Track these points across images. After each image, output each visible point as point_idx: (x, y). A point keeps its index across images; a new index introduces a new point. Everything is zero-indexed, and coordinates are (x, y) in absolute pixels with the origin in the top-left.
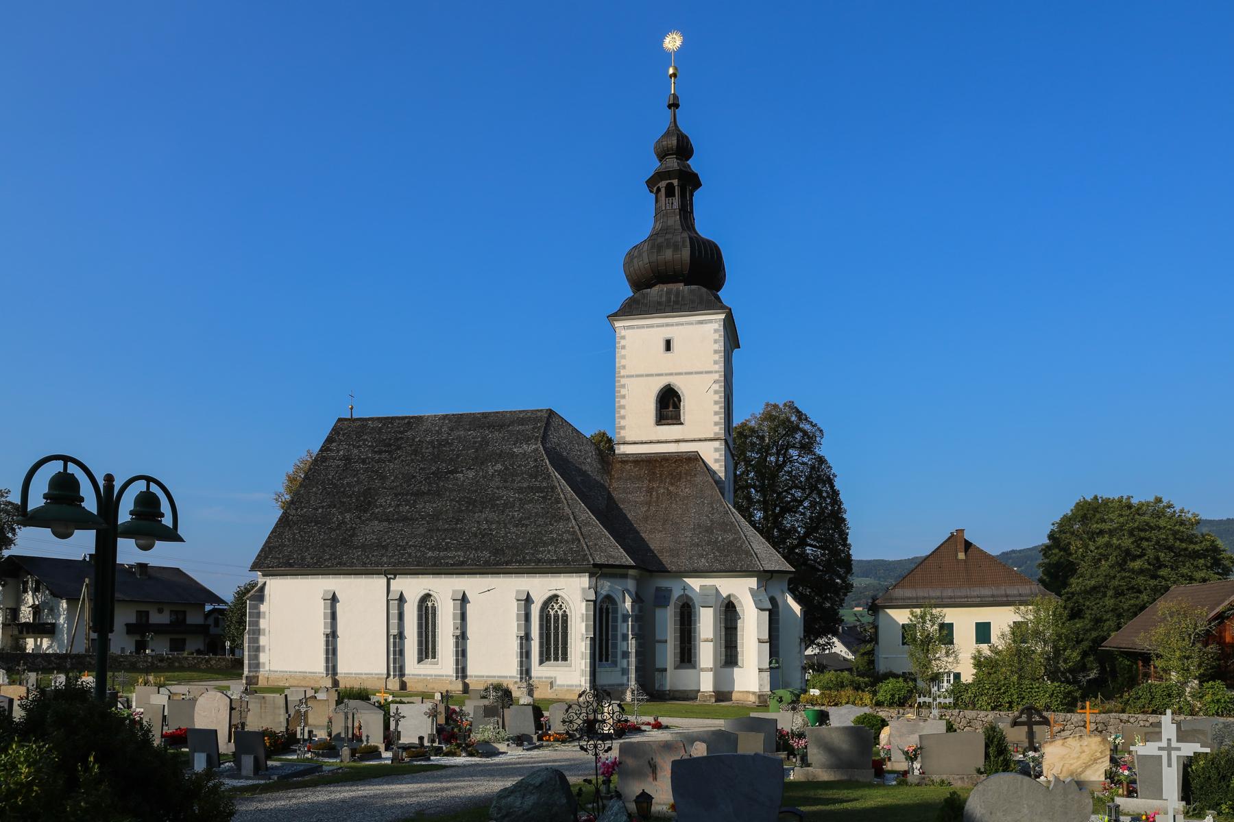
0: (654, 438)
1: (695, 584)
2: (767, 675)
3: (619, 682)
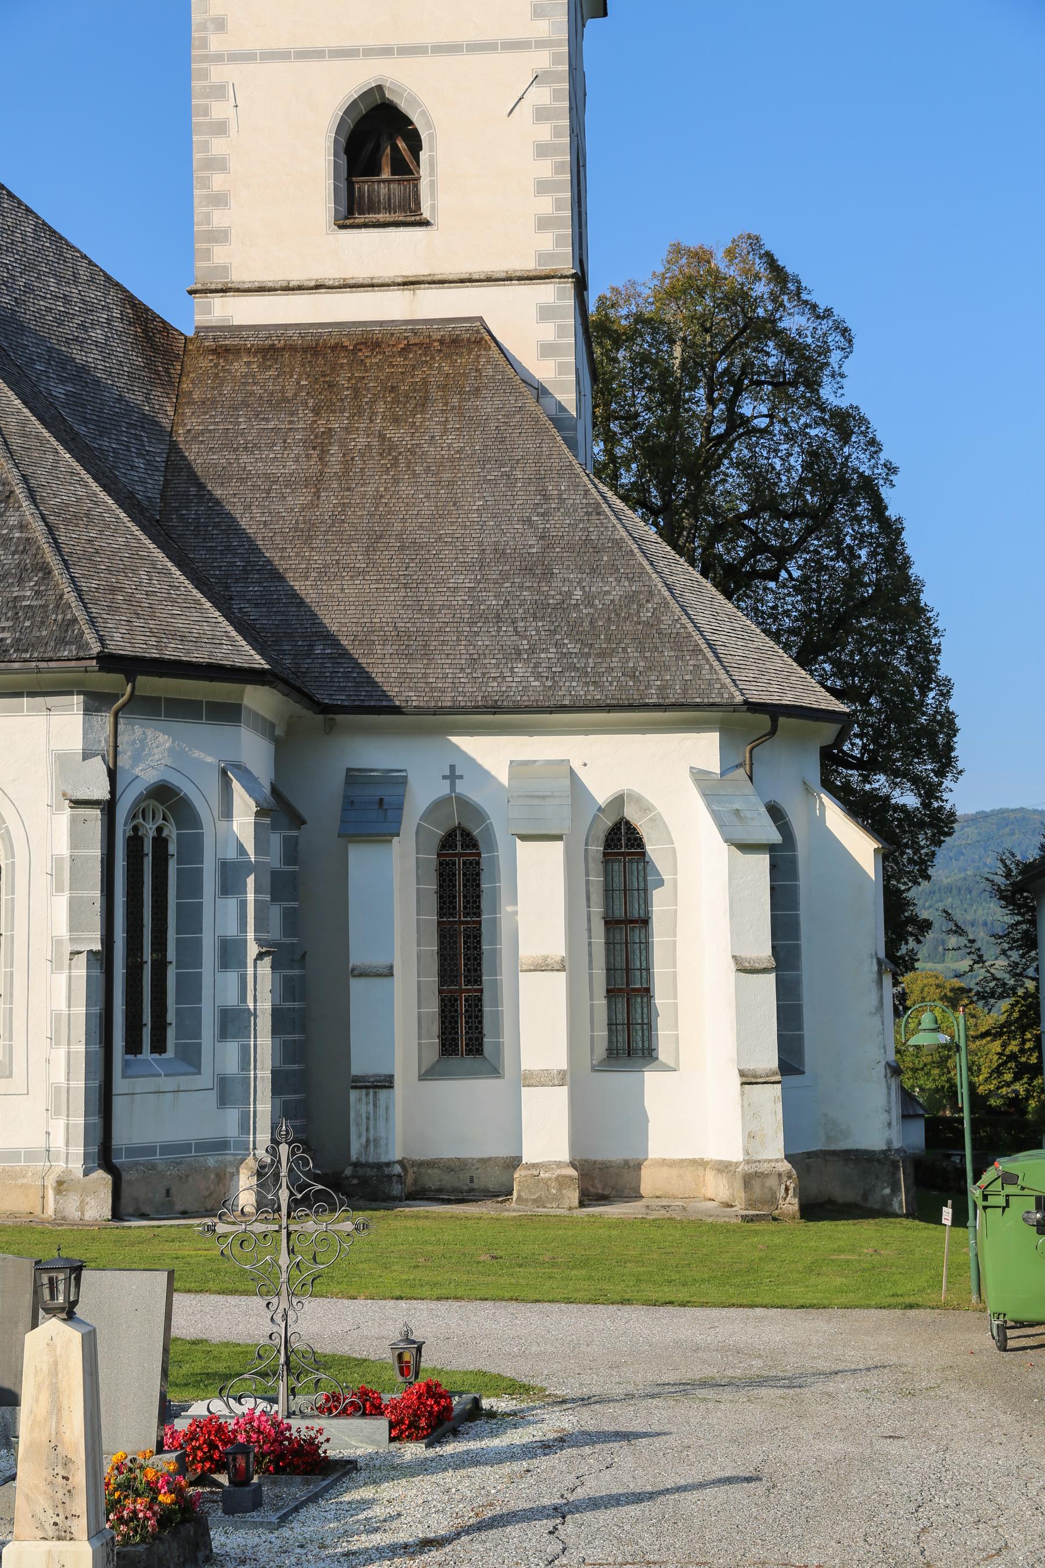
1: (494, 755)
2: (770, 1096)
3: (207, 1133)
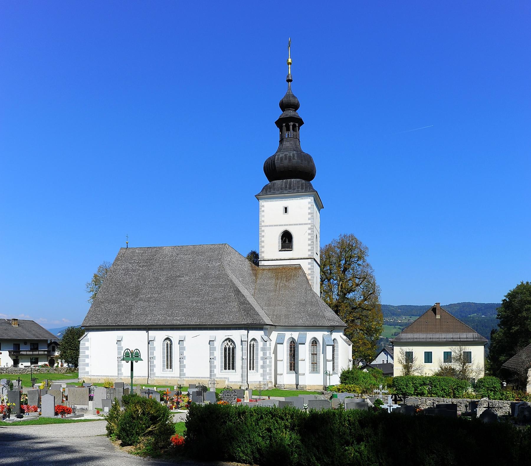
0: (278, 258)
